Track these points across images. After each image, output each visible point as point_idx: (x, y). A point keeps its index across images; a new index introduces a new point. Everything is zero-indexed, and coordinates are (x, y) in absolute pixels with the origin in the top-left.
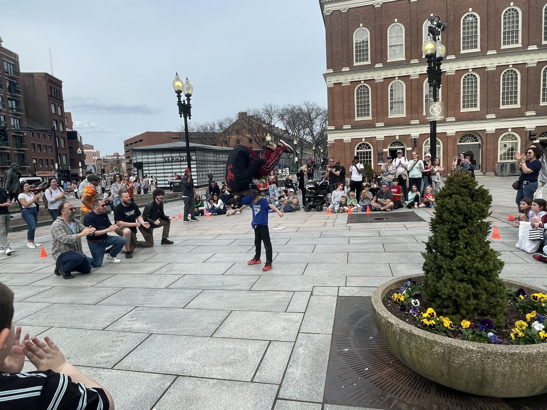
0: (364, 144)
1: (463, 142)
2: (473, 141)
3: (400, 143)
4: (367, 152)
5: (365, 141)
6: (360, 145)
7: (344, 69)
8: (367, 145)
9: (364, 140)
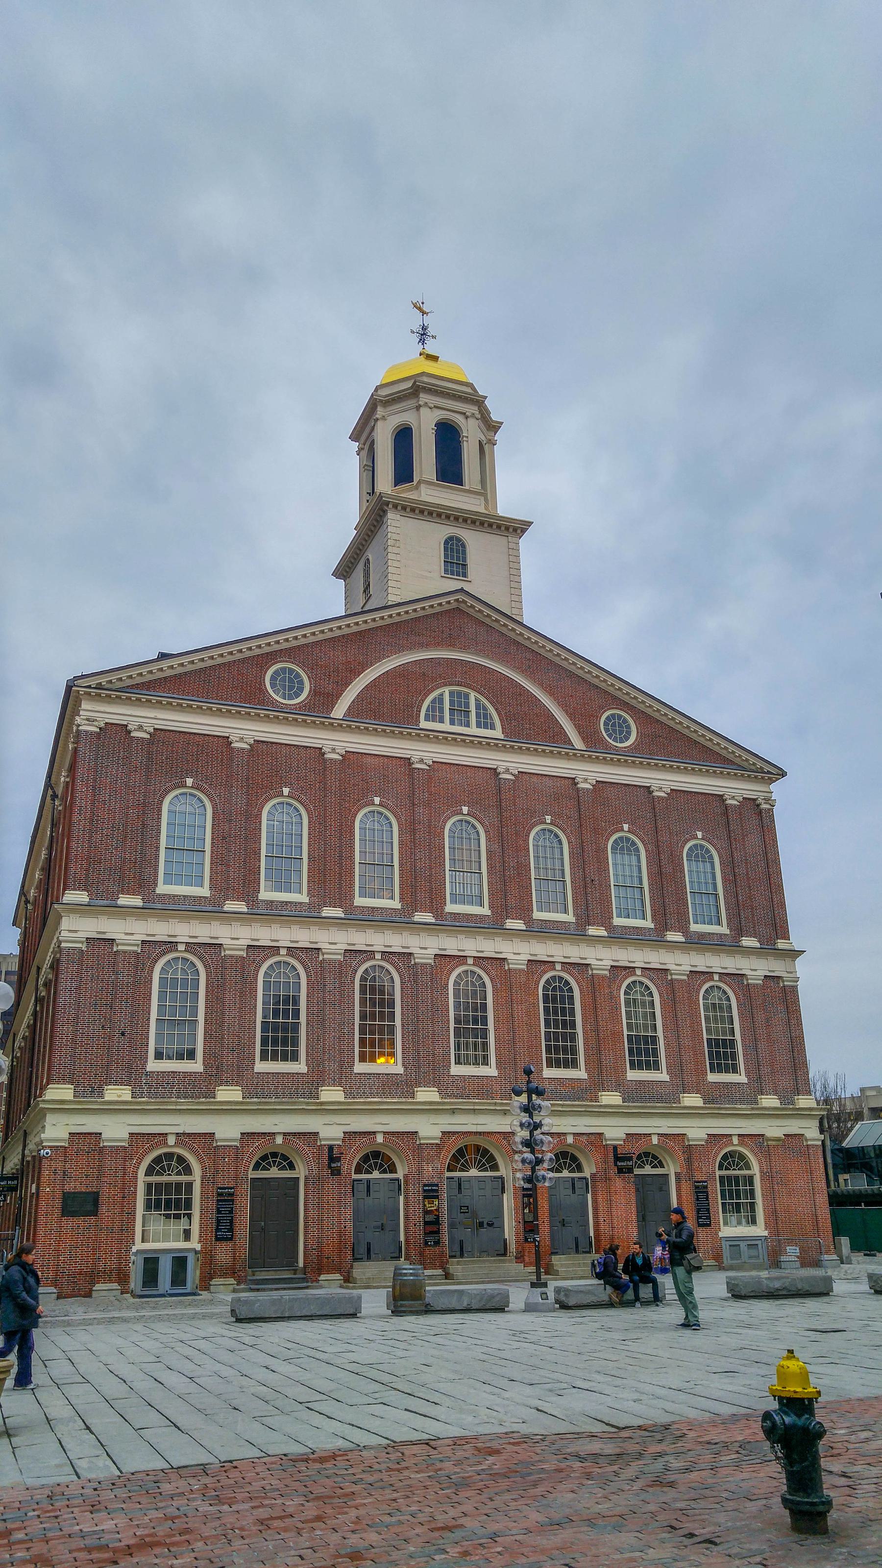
0: (169, 1156)
1: (461, 1170)
2: (486, 1170)
3: (285, 1158)
4: (179, 1185)
5: (176, 1145)
6: (158, 1160)
7: (124, 900)
8: (181, 1160)
9: (171, 1140)
